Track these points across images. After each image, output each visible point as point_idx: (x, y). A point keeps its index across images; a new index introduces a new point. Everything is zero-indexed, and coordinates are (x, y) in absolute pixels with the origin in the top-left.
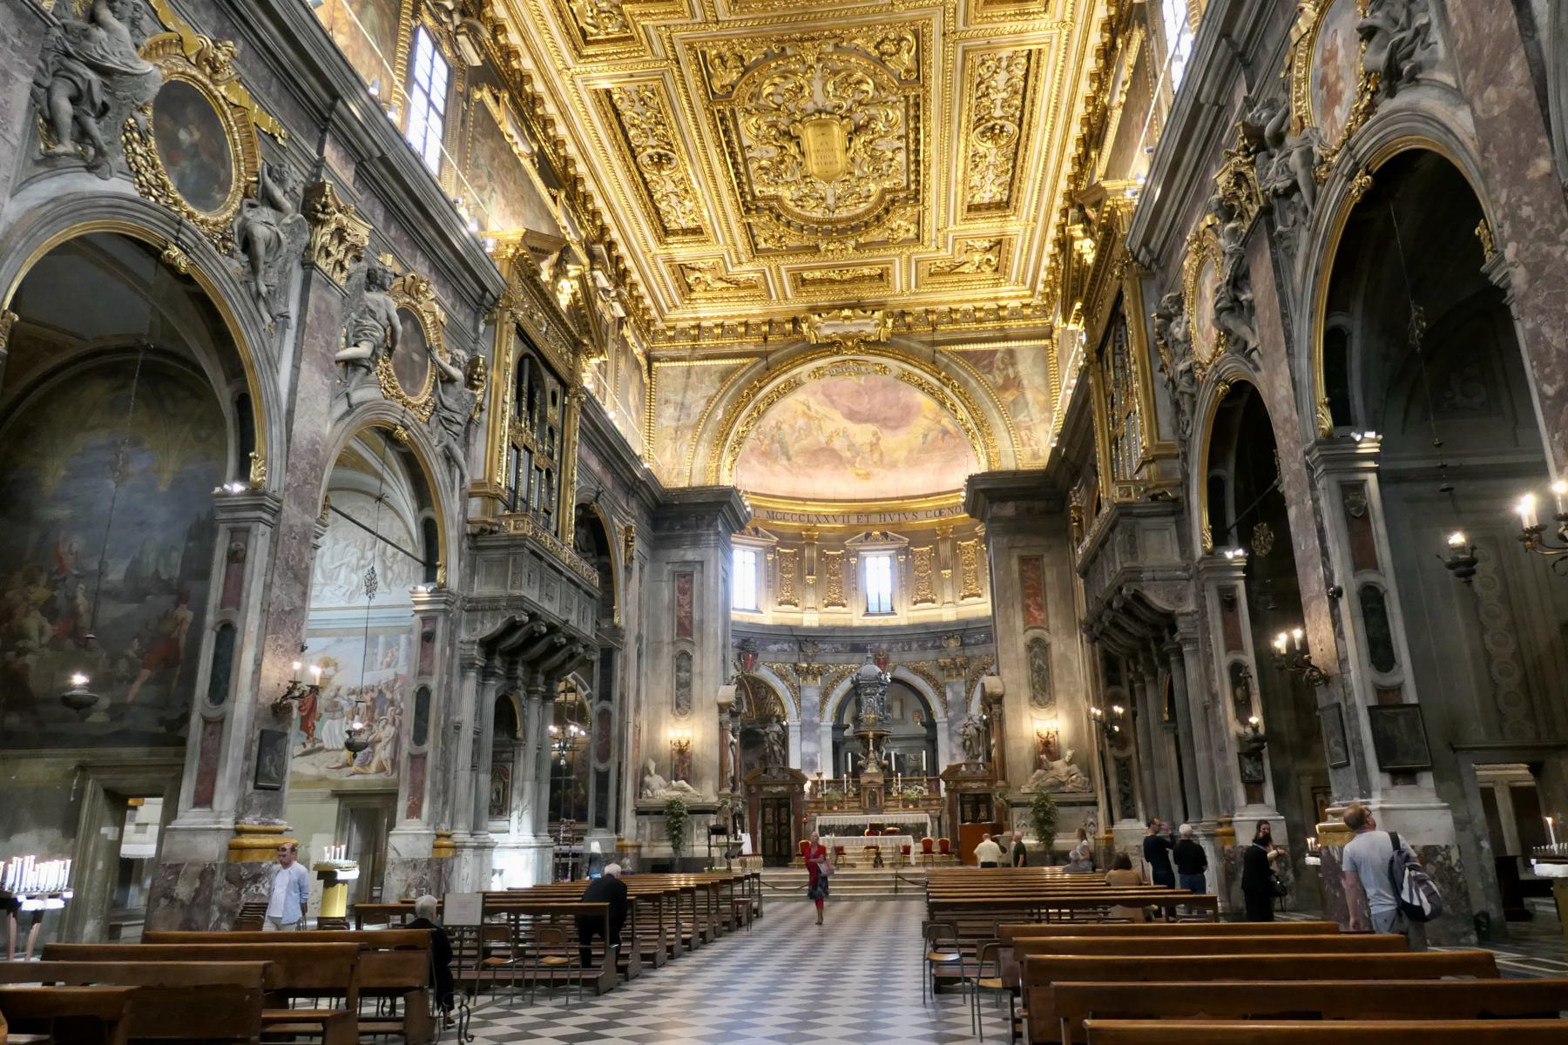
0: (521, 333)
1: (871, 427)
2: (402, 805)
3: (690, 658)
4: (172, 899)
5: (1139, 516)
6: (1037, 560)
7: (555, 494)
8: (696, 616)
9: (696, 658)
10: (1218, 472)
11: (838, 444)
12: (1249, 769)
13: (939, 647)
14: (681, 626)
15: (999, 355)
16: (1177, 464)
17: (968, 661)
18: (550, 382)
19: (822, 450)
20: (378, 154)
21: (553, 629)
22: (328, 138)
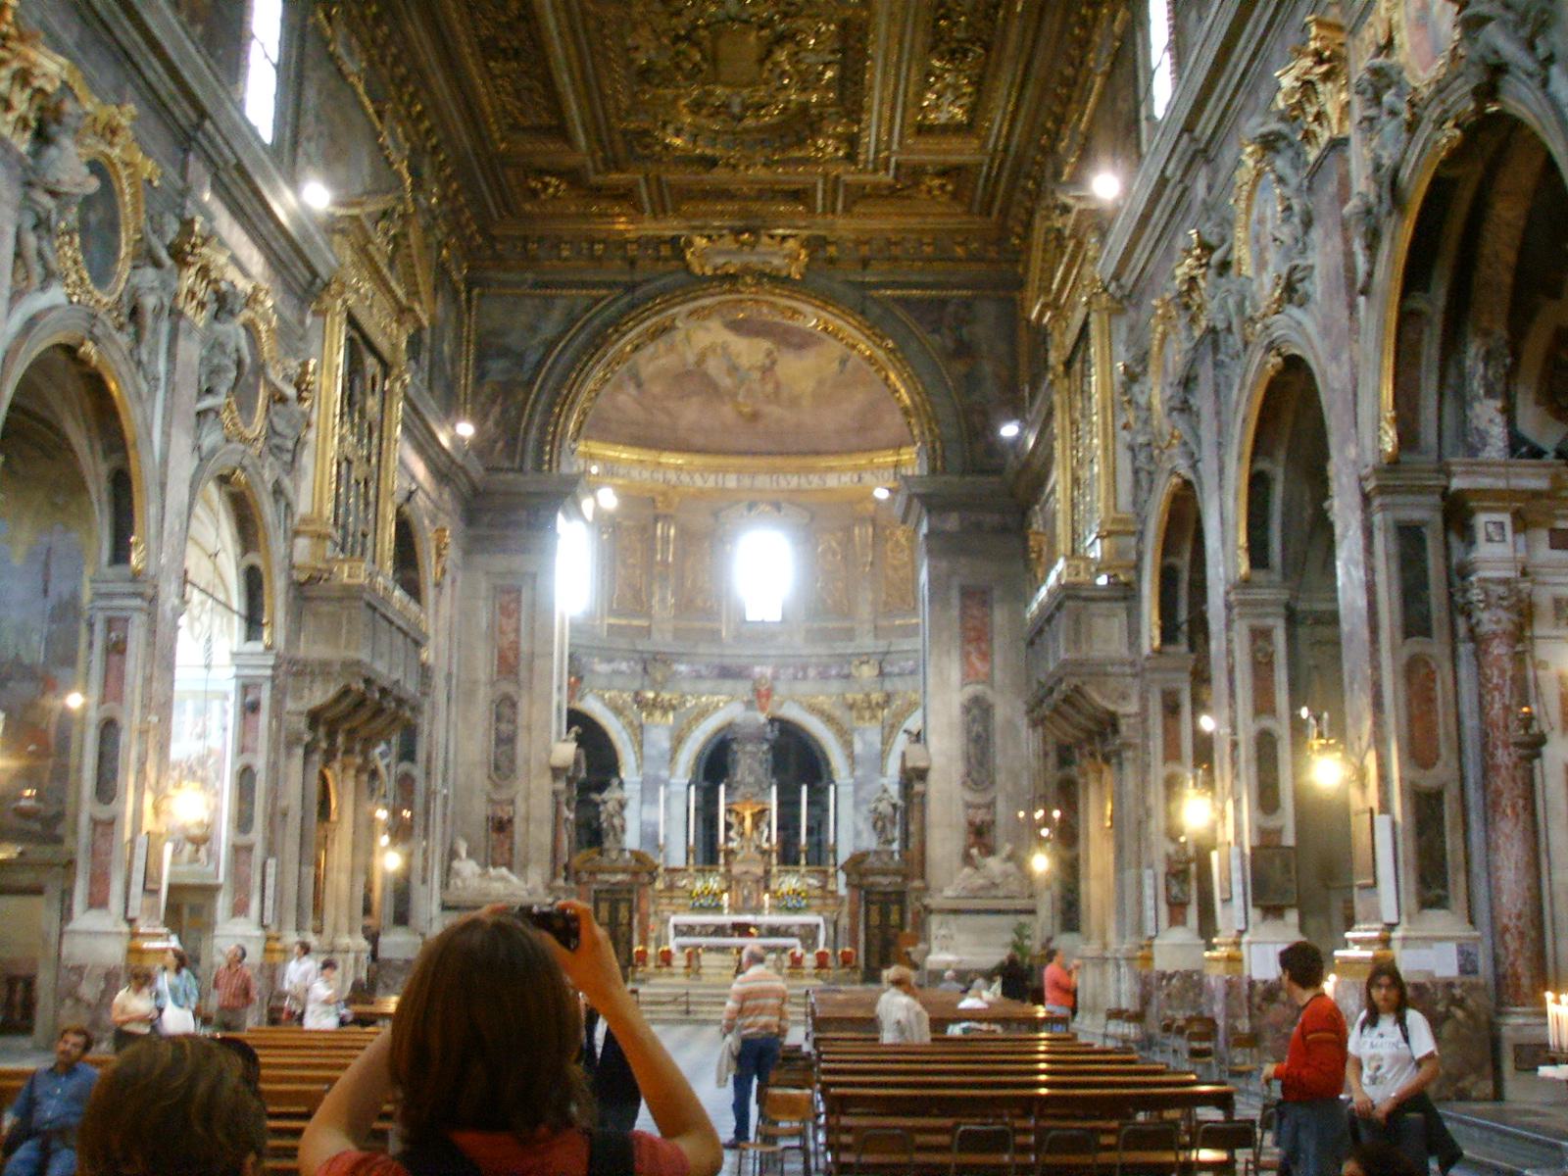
0: (352, 321)
1: (766, 344)
2: (223, 903)
3: (514, 705)
4: (78, 1000)
5: (1086, 599)
6: (984, 592)
7: (372, 510)
8: (524, 647)
9: (523, 705)
10: (1172, 560)
11: (714, 367)
12: (1175, 890)
13: (848, 677)
14: (502, 659)
15: (951, 309)
16: (1133, 541)
17: (888, 699)
18: (371, 363)
19: (688, 374)
20: (234, 161)
21: (384, 691)
22: (192, 157)
